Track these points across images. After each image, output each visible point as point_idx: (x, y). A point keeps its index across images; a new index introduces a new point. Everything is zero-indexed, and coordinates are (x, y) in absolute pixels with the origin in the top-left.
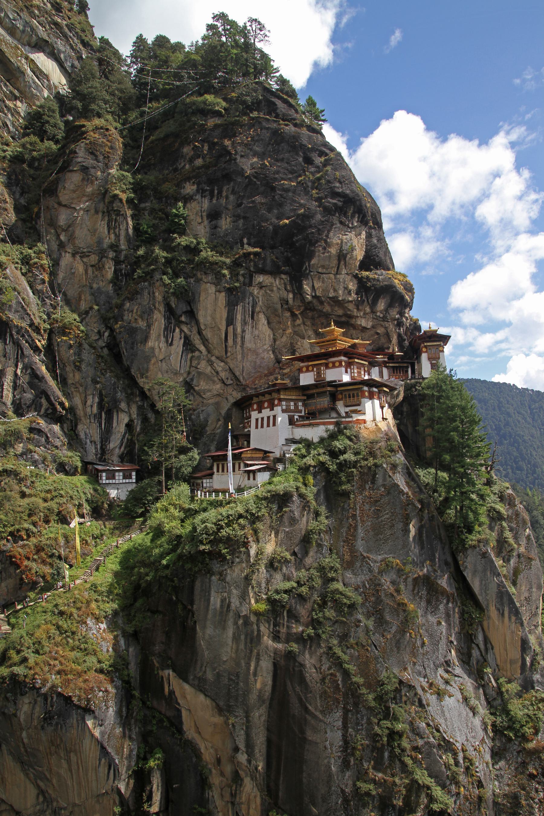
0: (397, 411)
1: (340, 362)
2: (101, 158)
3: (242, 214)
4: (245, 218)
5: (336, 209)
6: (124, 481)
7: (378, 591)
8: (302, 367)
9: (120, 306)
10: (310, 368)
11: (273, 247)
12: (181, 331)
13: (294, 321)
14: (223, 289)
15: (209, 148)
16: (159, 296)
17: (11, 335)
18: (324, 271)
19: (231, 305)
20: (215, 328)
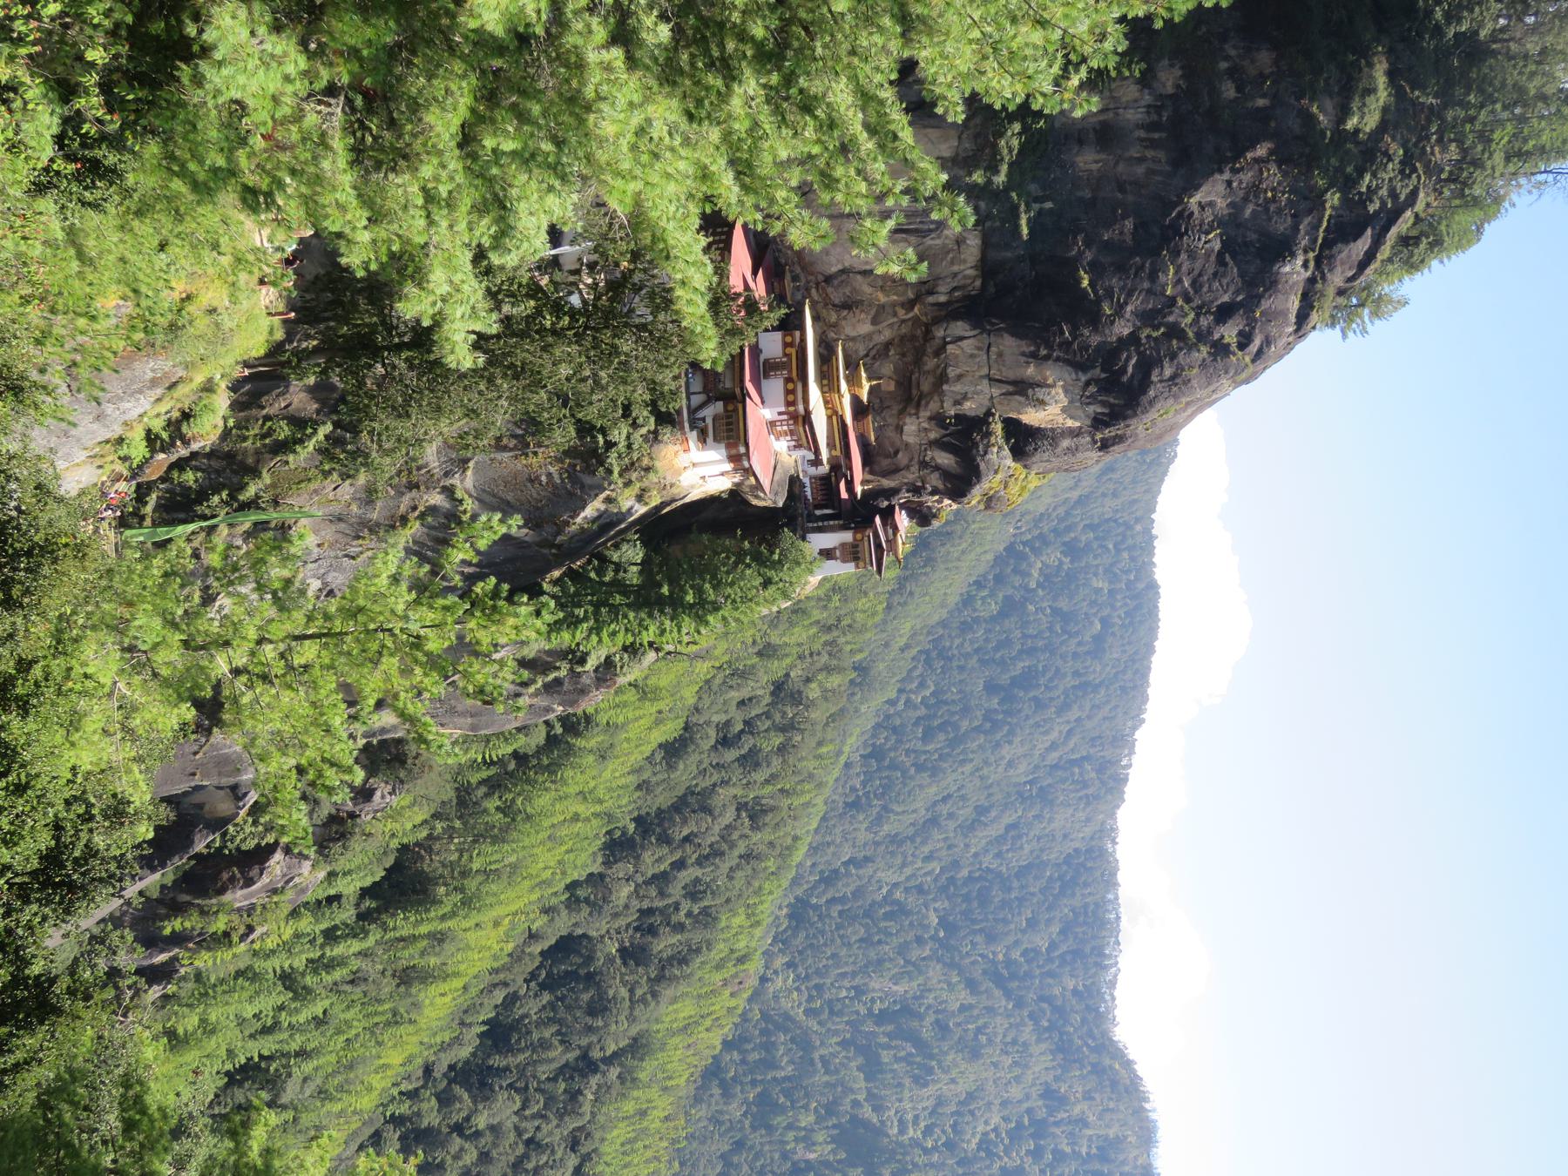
0: (735, 494)
1: (793, 403)
7: (417, 487)
10: (788, 350)
13: (903, 305)
15: (1258, 109)
18: (994, 357)
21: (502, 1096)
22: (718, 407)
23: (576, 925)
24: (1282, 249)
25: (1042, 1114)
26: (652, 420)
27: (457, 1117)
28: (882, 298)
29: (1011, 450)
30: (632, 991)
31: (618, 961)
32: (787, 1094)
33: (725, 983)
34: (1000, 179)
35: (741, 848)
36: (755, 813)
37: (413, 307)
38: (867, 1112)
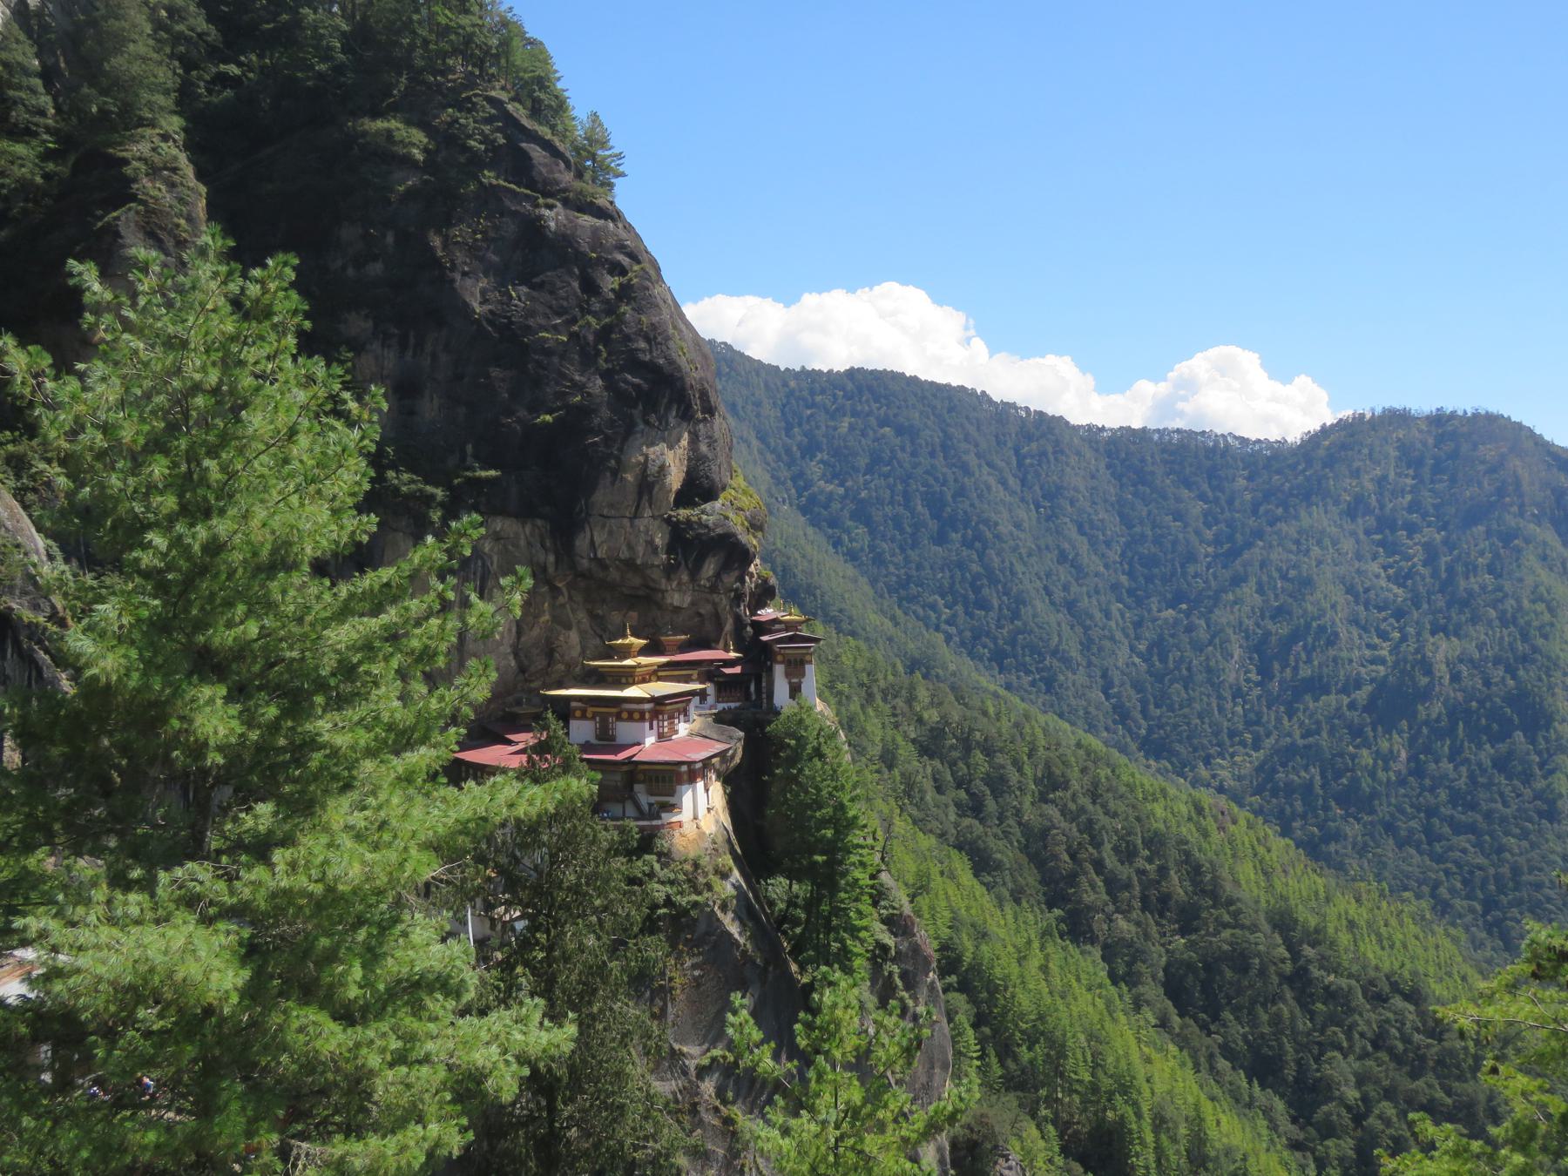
0: (727, 779)
1: (642, 713)
2: (170, 244)
7: (695, 1105)
10: (589, 715)
17: (17, 644)
21: (1328, 1070)
22: (637, 787)
23: (1154, 978)
24: (533, 228)
25: (1371, 521)
26: (647, 857)
27: (1347, 1119)
28: (546, 617)
30: (1226, 926)
31: (1194, 937)
32: (1338, 775)
33: (1222, 828)
34: (439, 493)
35: (1085, 801)
36: (1051, 783)
37: (506, 1084)
38: (1362, 695)
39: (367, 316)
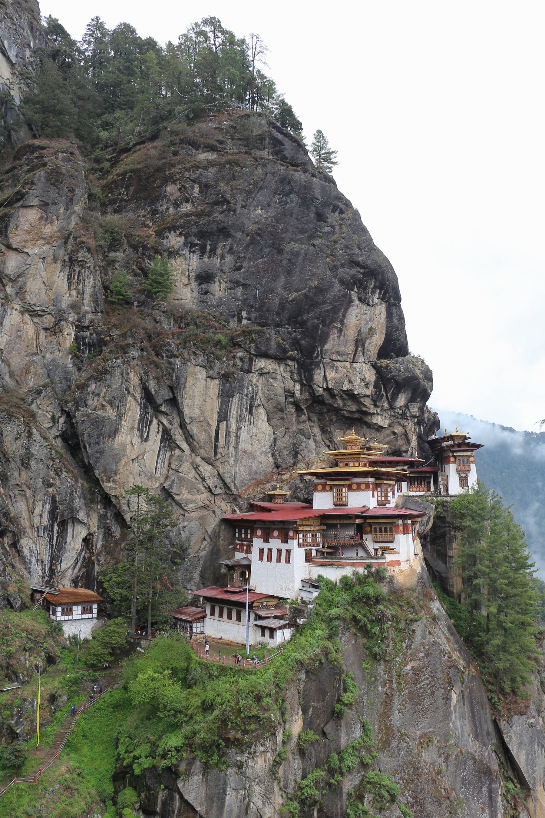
1: (367, 485)
3: (242, 281)
4: (244, 285)
5: (355, 282)
6: (83, 616)
8: (317, 485)
9: (82, 387)
10: (328, 488)
11: (278, 325)
12: (160, 423)
13: (298, 416)
14: (216, 375)
16: (134, 379)
18: (339, 358)
19: (226, 396)
20: (204, 423)
29: (398, 356)
39: (181, 234)
